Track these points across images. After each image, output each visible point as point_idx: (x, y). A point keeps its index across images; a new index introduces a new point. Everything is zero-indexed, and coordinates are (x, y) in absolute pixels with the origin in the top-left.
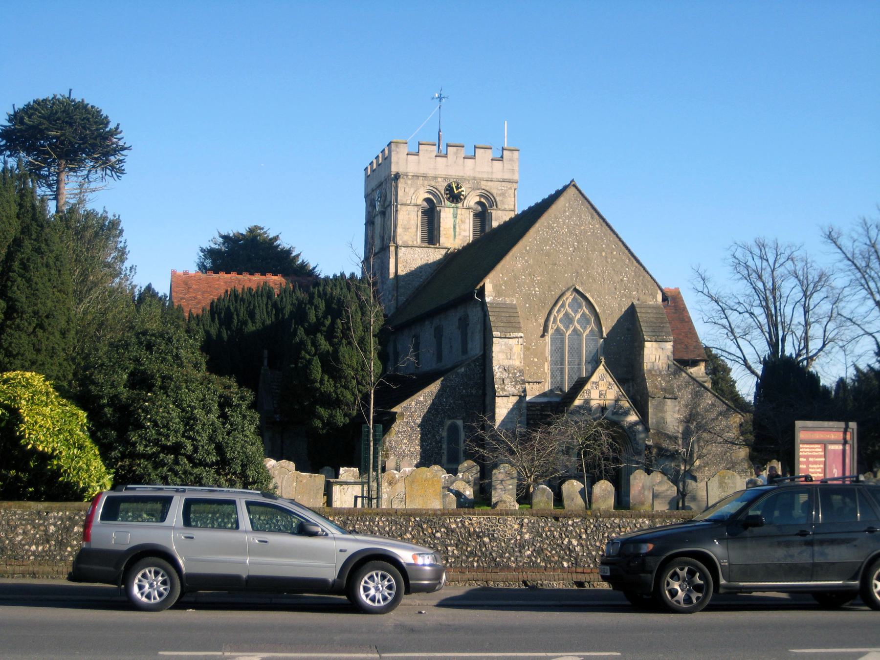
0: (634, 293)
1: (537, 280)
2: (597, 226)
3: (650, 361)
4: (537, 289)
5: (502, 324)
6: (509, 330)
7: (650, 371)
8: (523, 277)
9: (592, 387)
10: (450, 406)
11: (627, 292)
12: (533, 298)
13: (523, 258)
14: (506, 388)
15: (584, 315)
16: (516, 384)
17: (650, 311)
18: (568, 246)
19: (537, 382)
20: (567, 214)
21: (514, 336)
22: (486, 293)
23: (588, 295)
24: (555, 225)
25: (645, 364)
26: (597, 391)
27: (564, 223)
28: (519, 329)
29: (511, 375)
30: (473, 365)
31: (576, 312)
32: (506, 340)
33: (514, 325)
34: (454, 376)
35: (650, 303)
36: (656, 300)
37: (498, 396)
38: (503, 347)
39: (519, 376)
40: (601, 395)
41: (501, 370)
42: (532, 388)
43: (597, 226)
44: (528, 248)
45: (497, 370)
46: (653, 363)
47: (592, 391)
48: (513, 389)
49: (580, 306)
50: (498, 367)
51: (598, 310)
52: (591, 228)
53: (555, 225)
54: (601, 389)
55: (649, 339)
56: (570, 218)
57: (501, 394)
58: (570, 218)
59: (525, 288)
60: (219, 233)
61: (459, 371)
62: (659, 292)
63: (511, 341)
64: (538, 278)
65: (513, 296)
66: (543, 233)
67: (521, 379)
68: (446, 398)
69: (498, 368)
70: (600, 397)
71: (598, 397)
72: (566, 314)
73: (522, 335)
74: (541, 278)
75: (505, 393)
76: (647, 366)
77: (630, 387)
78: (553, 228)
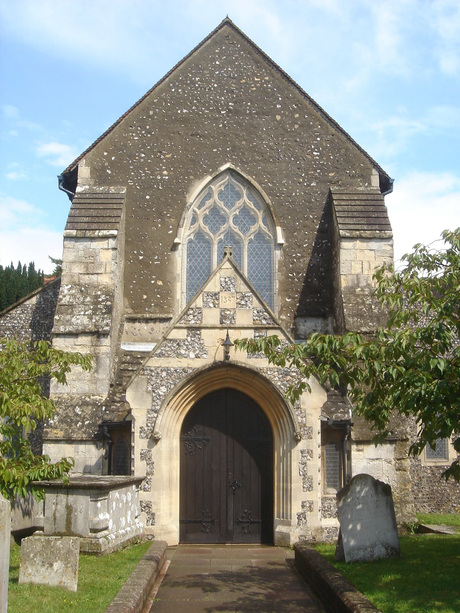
0: (331, 175)
1: (167, 159)
2: (267, 78)
3: (353, 272)
4: (165, 172)
5: (86, 219)
6: (94, 226)
7: (351, 290)
8: (143, 155)
9: (206, 303)
11: (319, 173)
12: (158, 186)
14: (74, 320)
15: (245, 210)
17: (356, 198)
20: (217, 63)
21: (100, 234)
22: (79, 181)
24: (197, 79)
25: (343, 278)
27: (212, 77)
28: (112, 225)
29: (88, 299)
30: (51, 294)
31: (230, 205)
32: (87, 244)
34: (18, 312)
35: (360, 189)
36: (370, 184)
39: (103, 301)
40: (223, 318)
42: (152, 329)
43: (267, 78)
44: (151, 113)
45: (66, 292)
46: (357, 275)
47: (205, 312)
48: (86, 320)
49: (239, 196)
50: (70, 286)
51: (269, 201)
52: (258, 82)
53: (197, 79)
54: (222, 305)
55: (348, 234)
56: (220, 68)
57: (62, 329)
58: (222, 68)
59: (144, 171)
60: (51, 258)
61: (27, 302)
62: (374, 172)
64: (167, 156)
65: (124, 183)
66: (176, 91)
67: (106, 305)
69: (69, 290)
70: (222, 323)
71: (218, 323)
72: (215, 210)
73: (115, 232)
74: (173, 156)
75: (69, 328)
76: (344, 283)
77: (327, 325)
78: (194, 83)
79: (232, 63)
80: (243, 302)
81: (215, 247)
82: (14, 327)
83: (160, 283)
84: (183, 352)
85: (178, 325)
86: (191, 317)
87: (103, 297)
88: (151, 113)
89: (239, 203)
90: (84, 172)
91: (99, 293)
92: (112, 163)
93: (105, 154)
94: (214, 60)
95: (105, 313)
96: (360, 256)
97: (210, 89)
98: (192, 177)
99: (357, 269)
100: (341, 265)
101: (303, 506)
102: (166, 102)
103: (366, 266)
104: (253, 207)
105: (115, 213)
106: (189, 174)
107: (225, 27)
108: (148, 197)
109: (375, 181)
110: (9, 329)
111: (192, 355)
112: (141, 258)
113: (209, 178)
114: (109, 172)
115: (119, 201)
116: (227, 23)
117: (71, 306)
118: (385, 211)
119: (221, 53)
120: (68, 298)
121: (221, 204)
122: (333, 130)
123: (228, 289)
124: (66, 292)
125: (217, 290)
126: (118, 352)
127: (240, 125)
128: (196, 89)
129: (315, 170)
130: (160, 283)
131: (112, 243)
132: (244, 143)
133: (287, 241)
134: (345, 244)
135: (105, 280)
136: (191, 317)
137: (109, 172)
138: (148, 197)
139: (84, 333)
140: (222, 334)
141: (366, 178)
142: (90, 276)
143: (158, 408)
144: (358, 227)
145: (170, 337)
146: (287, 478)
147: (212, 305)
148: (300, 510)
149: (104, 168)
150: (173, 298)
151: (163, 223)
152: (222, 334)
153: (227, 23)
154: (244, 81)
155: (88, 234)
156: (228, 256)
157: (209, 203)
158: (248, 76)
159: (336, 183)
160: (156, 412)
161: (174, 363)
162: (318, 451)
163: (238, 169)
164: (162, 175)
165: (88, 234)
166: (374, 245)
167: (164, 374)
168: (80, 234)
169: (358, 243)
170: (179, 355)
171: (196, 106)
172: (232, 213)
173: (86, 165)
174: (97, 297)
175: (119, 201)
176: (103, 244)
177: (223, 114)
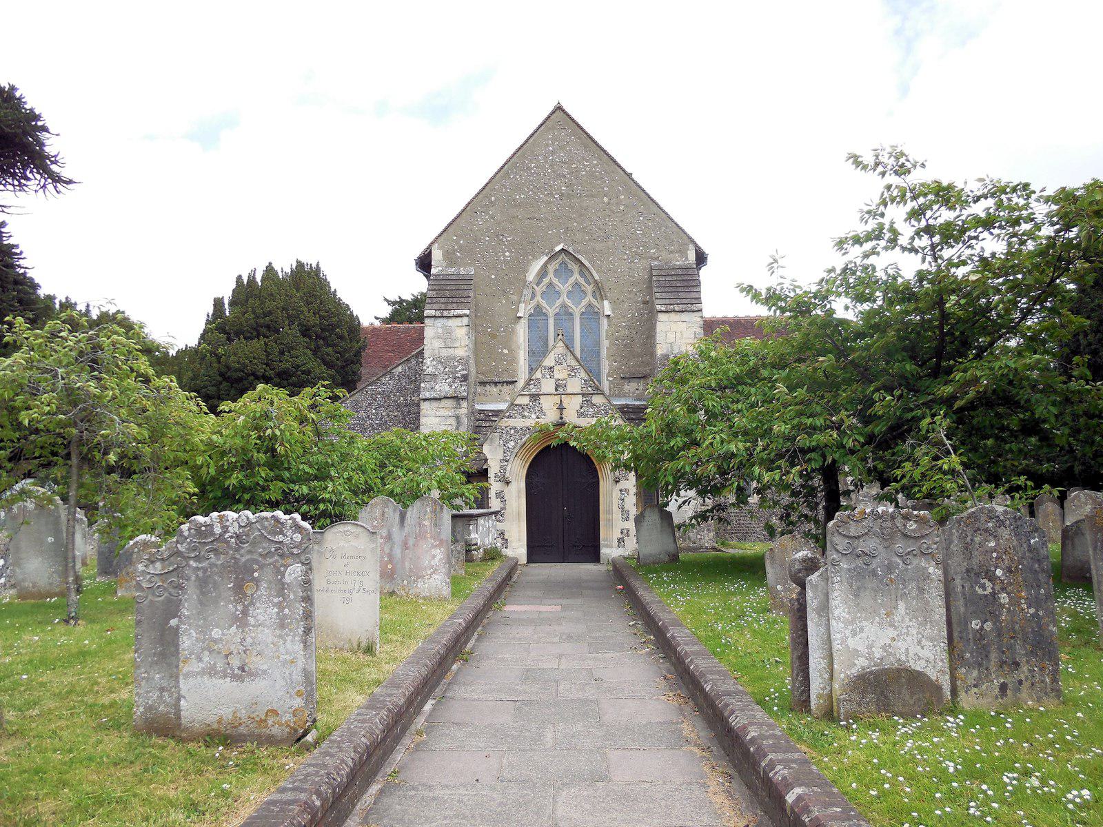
2: (595, 162)
4: (507, 254)
6: (450, 306)
8: (487, 239)
10: (381, 419)
13: (486, 213)
16: (454, 382)
18: (552, 193)
19: (503, 382)
23: (580, 257)
24: (533, 165)
26: (553, 381)
33: (462, 300)
36: (687, 258)
37: (425, 400)
38: (440, 331)
40: (557, 387)
41: (435, 363)
42: (501, 391)
43: (595, 162)
44: (493, 199)
45: (429, 363)
46: (671, 343)
47: (543, 381)
48: (447, 388)
54: (556, 376)
55: (663, 309)
56: (553, 153)
57: (428, 395)
61: (394, 371)
63: (451, 322)
68: (375, 409)
69: (431, 361)
70: (557, 390)
73: (467, 312)
74: (513, 239)
75: (434, 395)
78: (529, 169)
79: (562, 148)
80: (573, 374)
81: (551, 322)
82: (384, 391)
83: (506, 351)
84: (526, 414)
85: (522, 393)
86: (532, 386)
87: (460, 368)
88: (493, 199)
89: (571, 280)
90: (437, 256)
91: (456, 364)
92: (461, 247)
93: (455, 238)
94: (547, 145)
95: (463, 381)
96: (674, 327)
97: (544, 174)
98: (530, 257)
99: (671, 338)
100: (657, 335)
101: (622, 533)
102: (506, 188)
103: (678, 335)
104: (584, 283)
105: (466, 294)
106: (528, 255)
107: (558, 112)
108: (493, 277)
109: (692, 256)
110: (380, 394)
111: (534, 416)
112: (489, 330)
113: (545, 258)
114: (459, 255)
115: (468, 282)
116: (559, 108)
117: (433, 376)
118: (699, 285)
119: (554, 139)
120: (430, 369)
121: (556, 281)
122: (655, 209)
123: (561, 364)
124: (429, 363)
125: (552, 365)
126: (472, 412)
127: (572, 208)
128: (533, 174)
129: (638, 248)
130: (506, 351)
131: (465, 320)
132: (575, 224)
133: (613, 313)
134: (661, 317)
135: (461, 353)
136: (532, 386)
137: (459, 255)
138: (493, 277)
139: (445, 398)
140: (557, 399)
141: (683, 253)
142: (448, 349)
143: (508, 458)
144: (672, 301)
145: (517, 402)
146: (609, 512)
147: (548, 377)
148: (620, 536)
149: (454, 251)
150: (517, 363)
151: (507, 299)
152: (557, 399)
153: (559, 108)
154: (575, 166)
155: (446, 313)
156: (560, 336)
157: (546, 281)
158: (578, 161)
159: (657, 259)
160: (507, 461)
161: (518, 423)
162: (633, 490)
163: (571, 250)
164: (504, 256)
165: (446, 313)
166: (685, 316)
167: (512, 431)
168: (438, 314)
169: (672, 315)
170: (523, 417)
171: (532, 191)
172: (564, 288)
173: (439, 248)
174: (455, 367)
175: (468, 282)
176: (458, 321)
177: (556, 198)
